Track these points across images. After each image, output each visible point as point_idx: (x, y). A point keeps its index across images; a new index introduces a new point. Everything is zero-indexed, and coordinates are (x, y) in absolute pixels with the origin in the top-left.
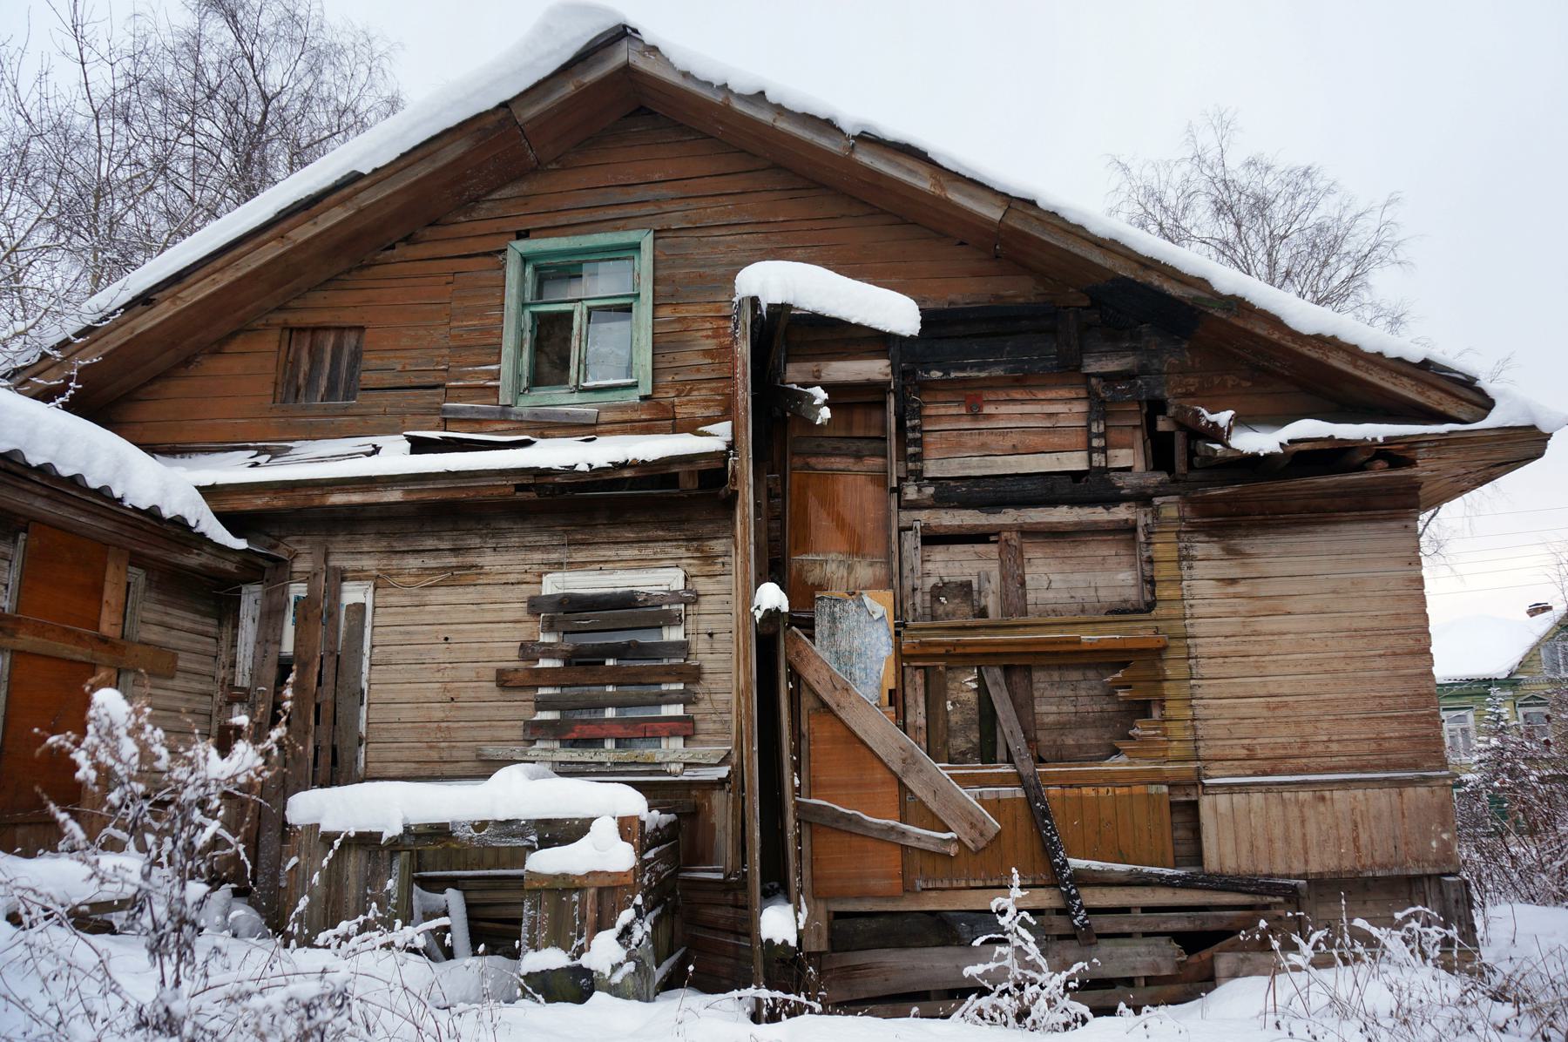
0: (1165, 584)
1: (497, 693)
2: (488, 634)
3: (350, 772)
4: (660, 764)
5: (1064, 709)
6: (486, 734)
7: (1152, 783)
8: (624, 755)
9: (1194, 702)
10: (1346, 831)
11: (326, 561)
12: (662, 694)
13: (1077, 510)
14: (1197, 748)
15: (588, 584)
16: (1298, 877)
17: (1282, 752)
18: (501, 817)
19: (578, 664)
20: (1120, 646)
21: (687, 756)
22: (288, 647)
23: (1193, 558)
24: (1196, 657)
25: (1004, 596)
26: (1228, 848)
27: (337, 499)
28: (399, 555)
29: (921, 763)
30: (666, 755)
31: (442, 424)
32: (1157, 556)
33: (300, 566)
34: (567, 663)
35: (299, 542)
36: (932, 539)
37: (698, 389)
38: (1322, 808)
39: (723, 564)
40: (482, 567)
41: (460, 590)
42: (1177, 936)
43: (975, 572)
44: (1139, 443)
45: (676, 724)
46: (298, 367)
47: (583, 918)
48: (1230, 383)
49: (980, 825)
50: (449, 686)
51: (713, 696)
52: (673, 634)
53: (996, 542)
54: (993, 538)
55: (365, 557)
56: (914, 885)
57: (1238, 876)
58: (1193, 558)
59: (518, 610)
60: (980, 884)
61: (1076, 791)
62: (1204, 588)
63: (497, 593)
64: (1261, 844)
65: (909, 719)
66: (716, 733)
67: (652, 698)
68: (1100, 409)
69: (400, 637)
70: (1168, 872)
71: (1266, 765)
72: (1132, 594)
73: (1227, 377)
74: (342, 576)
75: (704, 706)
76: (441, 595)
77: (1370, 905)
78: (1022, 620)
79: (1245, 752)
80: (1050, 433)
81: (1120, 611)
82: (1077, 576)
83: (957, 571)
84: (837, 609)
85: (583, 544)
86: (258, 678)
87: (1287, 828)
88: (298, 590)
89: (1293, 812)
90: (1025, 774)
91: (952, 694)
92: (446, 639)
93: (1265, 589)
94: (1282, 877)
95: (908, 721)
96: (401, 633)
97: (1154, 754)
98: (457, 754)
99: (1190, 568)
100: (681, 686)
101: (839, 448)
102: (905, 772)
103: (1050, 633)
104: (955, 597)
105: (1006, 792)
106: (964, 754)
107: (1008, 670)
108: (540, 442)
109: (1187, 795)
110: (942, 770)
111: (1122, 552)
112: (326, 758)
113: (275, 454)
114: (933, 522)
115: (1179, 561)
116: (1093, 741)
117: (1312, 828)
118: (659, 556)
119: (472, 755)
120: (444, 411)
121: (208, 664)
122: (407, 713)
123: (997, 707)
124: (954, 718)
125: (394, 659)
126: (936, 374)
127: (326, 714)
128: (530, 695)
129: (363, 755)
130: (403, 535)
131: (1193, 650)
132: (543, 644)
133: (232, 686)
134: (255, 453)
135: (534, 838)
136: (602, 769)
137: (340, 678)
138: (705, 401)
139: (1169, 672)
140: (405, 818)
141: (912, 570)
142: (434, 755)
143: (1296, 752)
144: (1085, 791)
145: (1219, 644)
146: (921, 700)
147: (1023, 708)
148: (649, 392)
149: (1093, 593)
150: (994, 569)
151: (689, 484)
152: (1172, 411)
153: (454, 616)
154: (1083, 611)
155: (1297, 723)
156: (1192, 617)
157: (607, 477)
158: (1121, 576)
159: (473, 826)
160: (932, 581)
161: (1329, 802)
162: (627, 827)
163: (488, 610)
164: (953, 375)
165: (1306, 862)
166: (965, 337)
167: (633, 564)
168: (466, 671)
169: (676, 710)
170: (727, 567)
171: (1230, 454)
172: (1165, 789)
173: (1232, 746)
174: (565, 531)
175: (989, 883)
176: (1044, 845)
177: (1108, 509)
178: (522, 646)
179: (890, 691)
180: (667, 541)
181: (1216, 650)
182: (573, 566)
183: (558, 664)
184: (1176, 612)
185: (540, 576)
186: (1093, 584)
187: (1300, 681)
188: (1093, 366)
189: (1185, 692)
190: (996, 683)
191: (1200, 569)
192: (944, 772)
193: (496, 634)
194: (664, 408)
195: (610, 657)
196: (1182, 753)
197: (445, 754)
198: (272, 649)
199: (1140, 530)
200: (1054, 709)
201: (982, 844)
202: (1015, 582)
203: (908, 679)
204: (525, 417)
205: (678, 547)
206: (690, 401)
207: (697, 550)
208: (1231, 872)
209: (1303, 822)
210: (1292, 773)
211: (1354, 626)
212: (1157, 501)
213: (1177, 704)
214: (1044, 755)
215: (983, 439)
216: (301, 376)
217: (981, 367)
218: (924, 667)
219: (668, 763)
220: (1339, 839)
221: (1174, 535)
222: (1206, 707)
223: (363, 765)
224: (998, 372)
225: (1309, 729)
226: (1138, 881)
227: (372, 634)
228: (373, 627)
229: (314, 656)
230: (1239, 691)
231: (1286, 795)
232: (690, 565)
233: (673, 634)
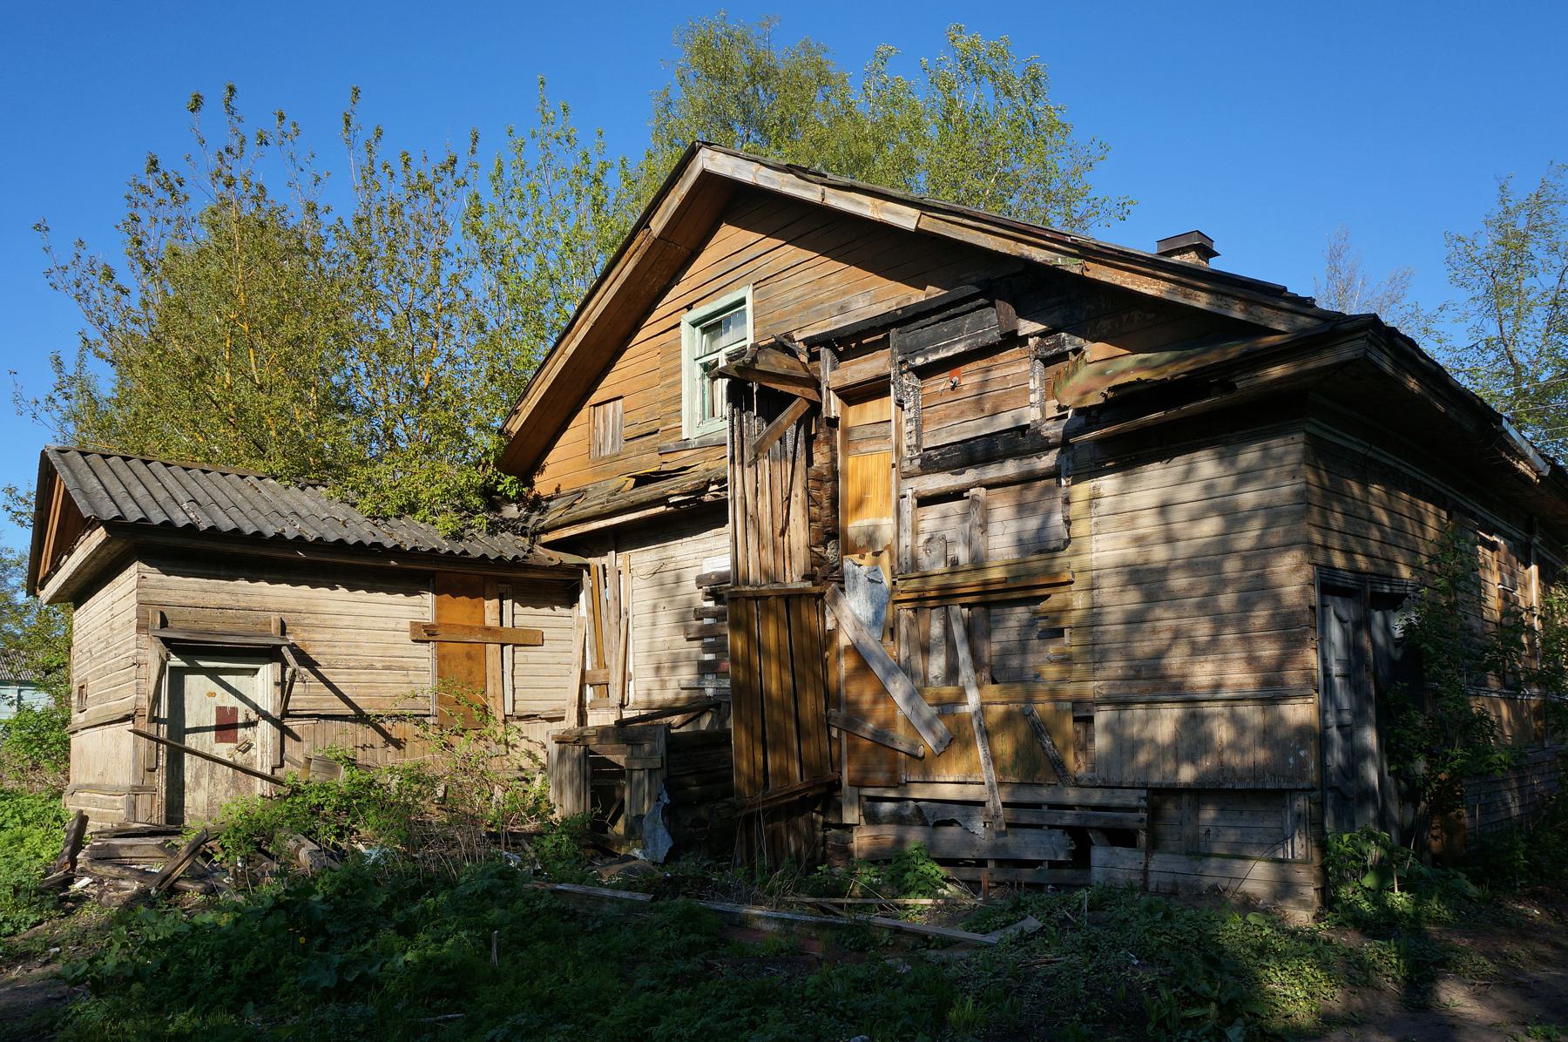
53: (967, 498)
120: (659, 449)
156: (1097, 551)
166: (938, 322)
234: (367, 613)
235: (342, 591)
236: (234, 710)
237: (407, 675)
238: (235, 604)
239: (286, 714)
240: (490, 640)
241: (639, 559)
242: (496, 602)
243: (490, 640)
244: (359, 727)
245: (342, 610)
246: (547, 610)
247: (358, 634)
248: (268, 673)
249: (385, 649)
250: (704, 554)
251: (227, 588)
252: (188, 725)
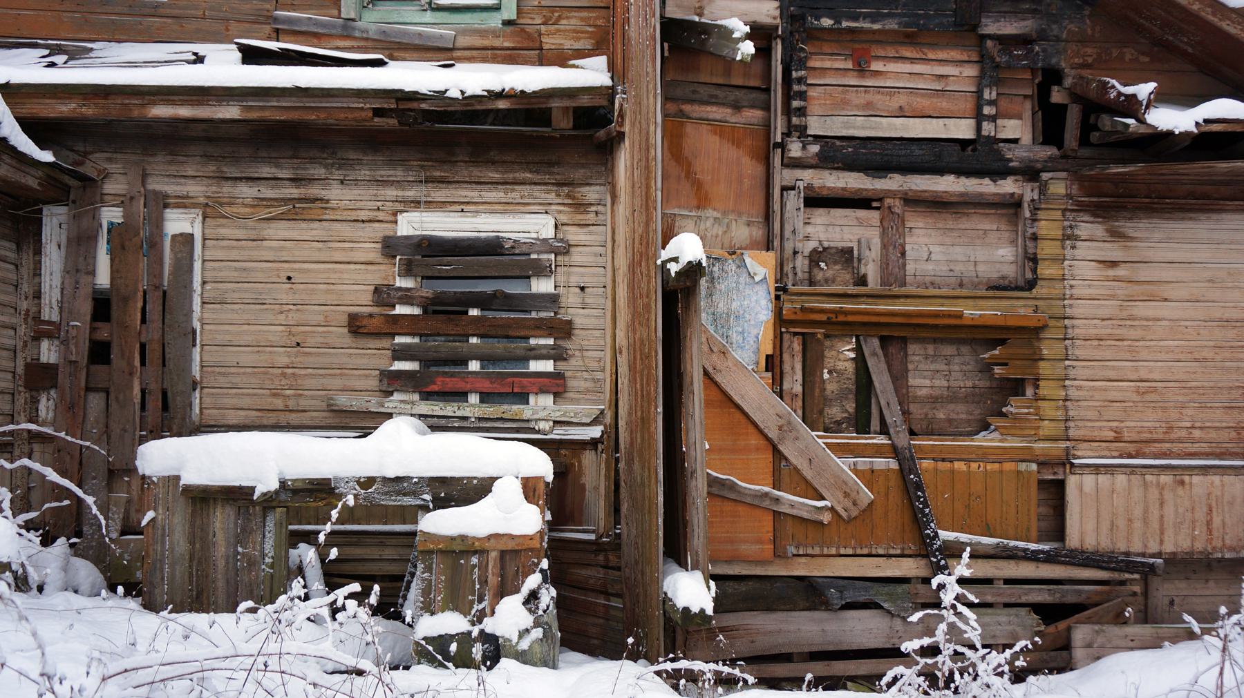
0: (1047, 263)
1: (348, 340)
2: (337, 276)
3: (184, 419)
4: (528, 421)
5: (937, 383)
6: (337, 383)
7: (1023, 461)
8: (490, 410)
9: (1067, 382)
10: (1201, 515)
11: (144, 183)
12: (532, 349)
13: (963, 180)
14: (1067, 429)
15: (448, 226)
16: (1153, 556)
17: (1148, 436)
18: (391, 474)
19: (435, 312)
20: (1001, 323)
21: (558, 414)
22: (103, 278)
23: (1077, 238)
24: (1072, 339)
25: (884, 265)
26: (1090, 526)
27: (162, 111)
28: (230, 182)
29: (798, 431)
30: (535, 412)
31: (274, 35)
32: (1042, 233)
33: (111, 187)
34: (425, 312)
35: (110, 160)
36: (815, 201)
37: (568, 18)
38: (1180, 491)
39: (597, 213)
40: (328, 201)
41: (304, 225)
42: (1037, 608)
43: (855, 238)
44: (1028, 114)
45: (546, 381)
47: (484, 582)
48: (1128, 57)
49: (853, 495)
50: (294, 329)
51: (585, 354)
52: (542, 286)
54: (875, 204)
55: (191, 181)
56: (785, 553)
57: (1096, 553)
58: (1077, 238)
59: (371, 251)
60: (850, 551)
61: (948, 465)
62: (1086, 269)
63: (346, 230)
64: (1121, 523)
65: (786, 386)
66: (587, 391)
67: (520, 352)
68: (990, 72)
69: (236, 274)
70: (1033, 546)
71: (1131, 448)
72: (1010, 271)
73: (1125, 50)
74: (163, 202)
75: (575, 363)
76: (281, 229)
77: (1211, 584)
78: (903, 291)
79: (1113, 434)
80: (938, 97)
81: (1000, 287)
82: (958, 249)
83: (838, 236)
84: (716, 269)
85: (442, 182)
86: (70, 312)
87: (1146, 511)
88: (111, 215)
89: (1154, 494)
90: (900, 446)
91: (829, 363)
92: (289, 278)
93: (1144, 273)
94: (1138, 555)
95: (785, 387)
96: (236, 269)
97: (1027, 432)
98: (304, 403)
99: (1073, 247)
100: (551, 341)
101: (716, 97)
102: (781, 439)
103: (931, 305)
104: (835, 263)
105: (880, 463)
106: (838, 423)
107: (884, 341)
108: (391, 63)
109: (1055, 473)
110: (818, 439)
111: (1003, 227)
112: (154, 403)
113: (74, 55)
114: (817, 183)
115: (1063, 240)
116: (963, 416)
117: (1169, 511)
118: (526, 201)
119: (324, 405)
120: (276, 20)
121: (10, 294)
122: (247, 357)
123: (874, 378)
124: (831, 387)
125: (229, 297)
126: (827, 22)
127: (153, 354)
128: (385, 343)
129: (198, 401)
130: (235, 160)
131: (1070, 331)
132: (400, 289)
133: (37, 319)
134: (46, 52)
135: (427, 497)
136: (465, 424)
137: (168, 317)
138: (575, 31)
139: (1045, 352)
140: (281, 473)
141: (794, 232)
142: (279, 403)
143: (1161, 436)
144: (957, 465)
145: (1095, 326)
146: (799, 367)
147: (899, 378)
148: (514, 17)
149: (972, 268)
150: (874, 237)
151: (563, 123)
152: (1068, 82)
153: (297, 253)
154: (961, 285)
155: (1164, 409)
156: (1071, 298)
157: (479, 107)
158: (1002, 252)
159: (358, 482)
160: (812, 245)
161: (1187, 487)
162: (530, 488)
163: (336, 249)
164: (844, 24)
165: (1162, 542)
167: (497, 207)
168: (314, 314)
169: (547, 366)
170: (601, 217)
171: (1143, 130)
172: (1034, 467)
173: (1100, 428)
174: (422, 167)
175: (859, 551)
176: (916, 516)
177: (995, 181)
178: (377, 290)
179: (767, 356)
180: (535, 184)
181: (1093, 332)
182: (430, 205)
183: (416, 311)
184: (1057, 292)
185: (395, 214)
186: (972, 259)
187: (1170, 368)
188: (991, 27)
189: (1060, 372)
190: (874, 354)
191: (1083, 249)
192: (820, 441)
193: (346, 276)
194: (529, 37)
195: (474, 306)
196: (1053, 433)
197: (291, 404)
198: (84, 279)
199: (1026, 205)
200: (927, 382)
201: (855, 513)
202: (894, 250)
203: (786, 345)
204: (371, 35)
205: (548, 192)
206: (559, 31)
207: (568, 196)
208: (1090, 549)
209: (1162, 504)
210: (1156, 456)
211: (1227, 316)
212: (1045, 176)
213: (1051, 383)
214: (916, 428)
215: (869, 97)
217: (874, 18)
218: (802, 334)
219: (536, 420)
220: (1194, 522)
221: (1059, 213)
222: (1079, 388)
223: (197, 411)
224: (892, 25)
225: (1174, 415)
226: (1004, 554)
227: (203, 269)
228: (204, 261)
229: (136, 290)
230: (1112, 374)
231: (1148, 478)
232: (560, 212)
233: (542, 286)
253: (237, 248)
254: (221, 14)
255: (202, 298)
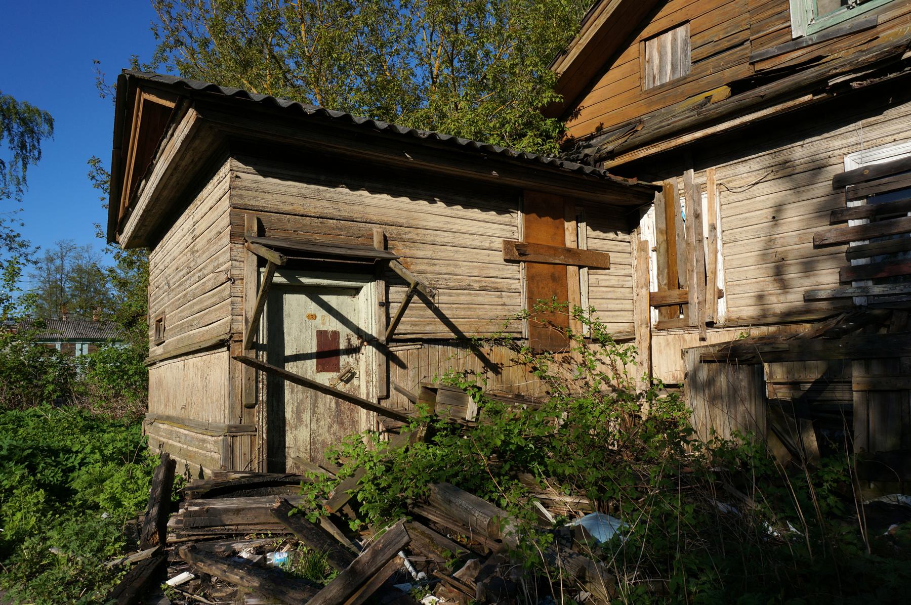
46: (653, 62)
69: (741, 222)
96: (741, 220)
216: (655, 68)
234: (464, 229)
235: (440, 206)
236: (336, 334)
237: (501, 297)
238: (336, 213)
239: (390, 339)
240: (571, 261)
241: (730, 172)
242: (574, 223)
243: (571, 261)
244: (460, 353)
245: (441, 225)
246: (611, 235)
247: (457, 252)
248: (371, 291)
249: (481, 268)
250: (844, 151)
251: (327, 195)
252: (288, 352)
253: (741, 206)
254: (720, 68)
255: (722, 241)
